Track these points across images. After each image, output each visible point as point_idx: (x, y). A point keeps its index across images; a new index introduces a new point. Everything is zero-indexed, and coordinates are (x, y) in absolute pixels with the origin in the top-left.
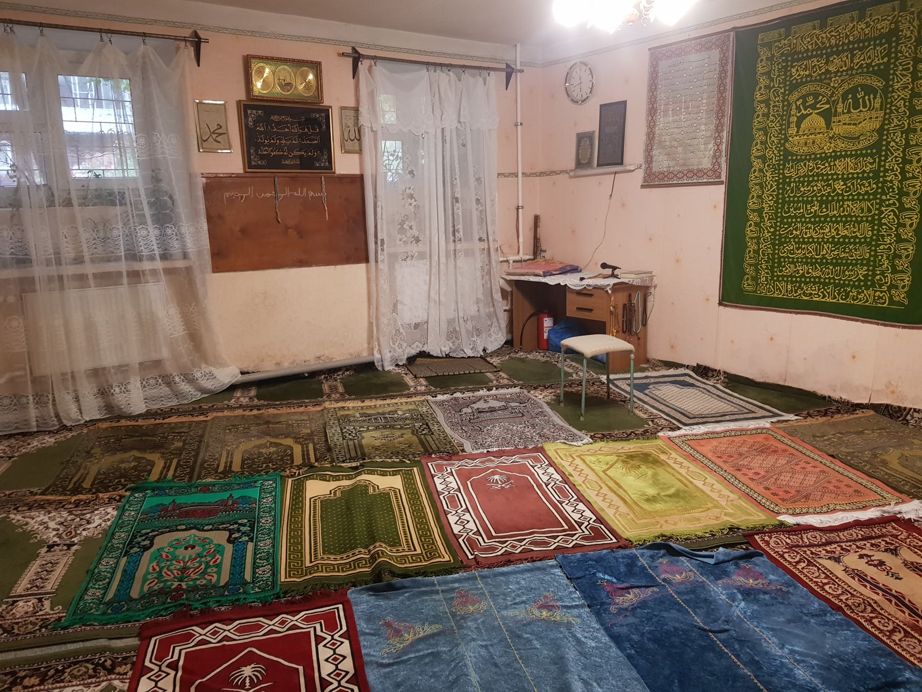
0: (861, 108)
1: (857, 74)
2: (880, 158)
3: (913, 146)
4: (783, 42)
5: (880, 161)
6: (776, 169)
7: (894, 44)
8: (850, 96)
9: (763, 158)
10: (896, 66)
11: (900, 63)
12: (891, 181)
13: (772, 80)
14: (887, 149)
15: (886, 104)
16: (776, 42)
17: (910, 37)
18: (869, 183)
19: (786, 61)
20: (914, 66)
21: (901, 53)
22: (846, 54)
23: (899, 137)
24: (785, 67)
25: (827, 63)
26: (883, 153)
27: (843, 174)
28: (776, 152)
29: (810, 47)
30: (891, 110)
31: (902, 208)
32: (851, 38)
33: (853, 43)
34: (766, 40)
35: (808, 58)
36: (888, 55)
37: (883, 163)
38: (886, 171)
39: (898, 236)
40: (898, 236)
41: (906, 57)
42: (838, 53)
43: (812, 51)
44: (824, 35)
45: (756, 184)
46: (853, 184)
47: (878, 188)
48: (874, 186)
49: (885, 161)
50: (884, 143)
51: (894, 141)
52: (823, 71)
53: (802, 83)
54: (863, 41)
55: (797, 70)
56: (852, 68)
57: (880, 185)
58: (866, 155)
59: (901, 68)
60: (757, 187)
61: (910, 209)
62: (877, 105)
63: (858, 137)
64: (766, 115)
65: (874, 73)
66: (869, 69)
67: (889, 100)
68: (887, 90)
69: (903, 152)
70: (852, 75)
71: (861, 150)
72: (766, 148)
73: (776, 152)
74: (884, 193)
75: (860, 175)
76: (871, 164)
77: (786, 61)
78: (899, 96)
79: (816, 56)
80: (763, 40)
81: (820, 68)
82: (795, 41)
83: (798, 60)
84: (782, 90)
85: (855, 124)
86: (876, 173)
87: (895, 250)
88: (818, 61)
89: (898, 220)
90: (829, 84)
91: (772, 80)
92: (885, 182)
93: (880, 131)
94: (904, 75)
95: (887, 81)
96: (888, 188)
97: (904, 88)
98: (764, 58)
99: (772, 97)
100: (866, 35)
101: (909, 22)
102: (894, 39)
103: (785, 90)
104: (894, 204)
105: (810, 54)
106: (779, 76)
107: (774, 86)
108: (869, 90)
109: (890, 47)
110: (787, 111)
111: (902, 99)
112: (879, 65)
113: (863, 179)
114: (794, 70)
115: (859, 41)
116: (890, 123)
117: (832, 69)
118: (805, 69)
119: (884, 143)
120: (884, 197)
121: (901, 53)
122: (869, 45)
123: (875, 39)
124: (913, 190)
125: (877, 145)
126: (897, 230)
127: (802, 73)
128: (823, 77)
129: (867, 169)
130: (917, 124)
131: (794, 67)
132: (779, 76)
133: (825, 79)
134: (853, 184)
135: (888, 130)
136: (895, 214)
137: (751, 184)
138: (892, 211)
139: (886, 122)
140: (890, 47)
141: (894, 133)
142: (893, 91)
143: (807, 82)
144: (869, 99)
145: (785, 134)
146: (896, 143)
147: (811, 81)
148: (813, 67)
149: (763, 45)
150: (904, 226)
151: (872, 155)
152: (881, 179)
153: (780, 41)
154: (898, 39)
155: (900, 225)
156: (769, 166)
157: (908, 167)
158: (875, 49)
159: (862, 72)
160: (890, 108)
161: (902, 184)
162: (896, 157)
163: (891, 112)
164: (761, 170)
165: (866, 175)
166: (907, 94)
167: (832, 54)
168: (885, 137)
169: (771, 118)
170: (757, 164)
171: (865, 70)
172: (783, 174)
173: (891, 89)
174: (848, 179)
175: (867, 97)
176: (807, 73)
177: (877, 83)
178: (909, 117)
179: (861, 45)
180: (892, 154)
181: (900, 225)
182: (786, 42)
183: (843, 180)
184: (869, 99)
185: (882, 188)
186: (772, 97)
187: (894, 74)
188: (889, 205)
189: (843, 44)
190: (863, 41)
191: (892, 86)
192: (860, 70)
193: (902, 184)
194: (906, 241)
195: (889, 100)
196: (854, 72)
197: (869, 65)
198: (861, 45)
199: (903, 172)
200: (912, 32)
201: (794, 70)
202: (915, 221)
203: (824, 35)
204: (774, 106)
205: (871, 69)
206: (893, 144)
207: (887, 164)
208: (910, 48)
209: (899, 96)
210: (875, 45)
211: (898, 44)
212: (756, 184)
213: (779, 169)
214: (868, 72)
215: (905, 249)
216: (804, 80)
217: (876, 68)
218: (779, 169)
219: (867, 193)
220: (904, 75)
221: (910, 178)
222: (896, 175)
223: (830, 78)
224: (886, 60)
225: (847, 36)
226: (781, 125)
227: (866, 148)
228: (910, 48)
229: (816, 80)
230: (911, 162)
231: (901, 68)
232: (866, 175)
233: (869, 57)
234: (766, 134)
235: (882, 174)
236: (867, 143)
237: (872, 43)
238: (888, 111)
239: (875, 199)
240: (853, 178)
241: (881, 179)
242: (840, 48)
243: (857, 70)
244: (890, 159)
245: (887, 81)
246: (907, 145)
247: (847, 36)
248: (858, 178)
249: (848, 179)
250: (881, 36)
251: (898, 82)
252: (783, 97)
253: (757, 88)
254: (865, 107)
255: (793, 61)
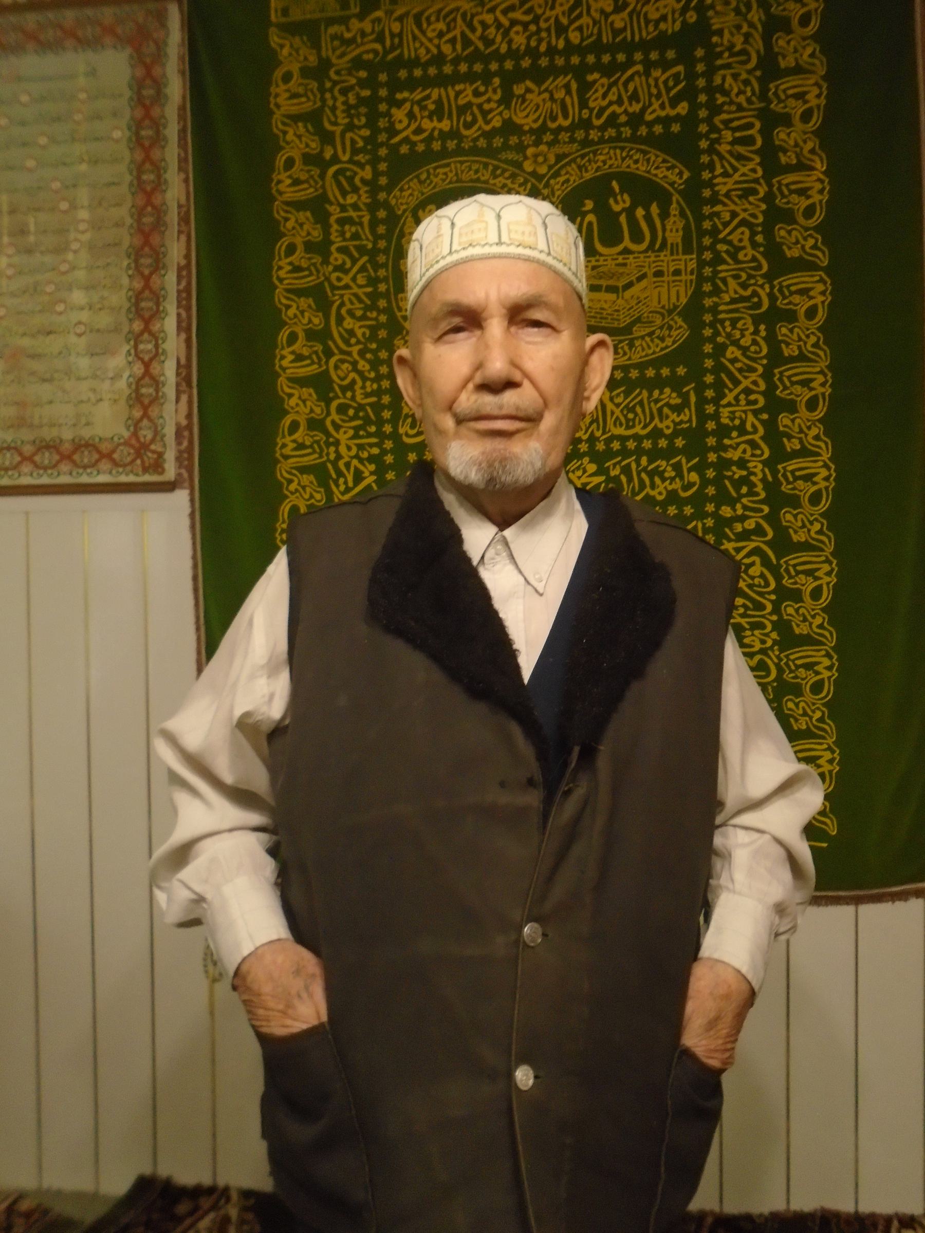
0: (627, 242)
1: (602, 141)
2: (701, 388)
3: (792, 359)
4: (355, 24)
5: (702, 401)
6: (367, 421)
7: (700, 68)
8: (589, 205)
9: (321, 384)
10: (713, 129)
11: (726, 123)
12: (742, 463)
13: (327, 138)
14: (719, 368)
15: (702, 233)
16: (331, 21)
17: (743, 52)
18: (677, 467)
19: (371, 83)
20: (766, 132)
21: (726, 93)
22: (561, 81)
23: (748, 333)
24: (371, 103)
25: (506, 100)
26: (709, 379)
27: (592, 440)
28: (363, 365)
29: (447, 49)
30: (717, 254)
31: (783, 544)
32: (575, 37)
33: (581, 50)
34: (296, 15)
35: (443, 81)
36: (689, 94)
37: (710, 409)
38: (723, 431)
39: (783, 626)
40: (783, 626)
41: (740, 108)
42: (538, 75)
43: (456, 61)
44: (489, 18)
45: (303, 470)
46: (626, 470)
47: (705, 482)
48: (694, 477)
49: (716, 401)
50: (708, 348)
51: (736, 343)
52: (497, 123)
53: (430, 156)
54: (612, 49)
55: (411, 115)
56: (586, 124)
57: (711, 474)
58: (658, 383)
59: (728, 135)
60: (306, 479)
61: (806, 547)
62: (675, 237)
63: (628, 330)
64: (320, 248)
65: (651, 140)
66: (634, 130)
67: (707, 225)
68: (695, 195)
69: (767, 375)
70: (586, 143)
71: (642, 366)
72: (329, 354)
73: (363, 365)
74: (723, 498)
75: (647, 444)
76: (678, 409)
77: (371, 83)
78: (734, 215)
79: (470, 77)
80: (285, 12)
81: (485, 113)
82: (396, 27)
83: (411, 84)
84: (367, 173)
85: (612, 289)
86: (695, 442)
87: (780, 670)
88: (477, 93)
89: (778, 578)
90: (519, 165)
91: (327, 138)
92: (723, 464)
93: (693, 312)
94: (740, 157)
95: (695, 168)
96: (738, 484)
97: (747, 193)
98: (295, 68)
99: (333, 192)
100: (616, 32)
101: (737, 11)
102: (700, 53)
103: (376, 174)
104: (759, 531)
105: (448, 69)
106: (350, 127)
107: (335, 159)
108: (645, 191)
109: (691, 76)
110: (388, 236)
111: (743, 223)
112: (666, 121)
113: (654, 454)
114: (399, 114)
115: (598, 47)
116: (716, 292)
117: (525, 118)
118: (438, 113)
119: (708, 348)
120: (726, 512)
121: (726, 93)
122: (630, 63)
123: (645, 46)
124: (806, 490)
125: (688, 353)
126: (776, 610)
127: (427, 124)
128: (498, 142)
129: (667, 426)
130: (796, 299)
131: (399, 104)
132: (350, 127)
133: (506, 147)
134: (626, 470)
135: (714, 310)
136: (766, 562)
137: (283, 471)
138: (756, 551)
139: (707, 287)
140: (691, 76)
141: (734, 322)
142: (714, 200)
143: (444, 153)
144: (648, 218)
145: (388, 311)
146: (745, 350)
147: (459, 151)
148: (462, 110)
149: (292, 29)
150: (796, 596)
151: (676, 384)
152: (712, 457)
153: (344, 21)
154: (712, 55)
155: (786, 594)
156: (342, 409)
157: (784, 420)
158: (647, 74)
159: (618, 138)
160: (712, 248)
161: (775, 473)
162: (747, 391)
163: (718, 260)
164: (315, 424)
165: (663, 443)
166: (755, 209)
167: (519, 75)
168: (708, 332)
169: (337, 258)
170: (300, 404)
171: (627, 132)
172: (395, 436)
173: (707, 193)
174: (609, 454)
175: (640, 212)
176: (445, 125)
177: (668, 173)
178: (770, 277)
179: (606, 58)
180: (736, 383)
181: (786, 594)
182: (367, 26)
183: (596, 457)
184: (648, 218)
185: (718, 481)
186: (333, 192)
187: (711, 150)
188: (745, 535)
189: (552, 51)
190: (612, 49)
191: (710, 184)
192: (611, 132)
193: (775, 473)
194: (808, 640)
195: (707, 225)
196: (594, 135)
197: (636, 120)
198: (606, 58)
199: (774, 436)
200: (747, 36)
201: (399, 114)
202: (827, 581)
203: (489, 18)
204: (342, 222)
205: (643, 131)
206: (732, 352)
207: (725, 412)
208: (746, 82)
209: (734, 215)
210: (648, 65)
211: (709, 74)
212: (303, 470)
213: (380, 422)
214: (634, 139)
215: (809, 667)
216: (436, 146)
217: (658, 129)
218: (380, 422)
219: (672, 497)
220: (740, 157)
221: (796, 454)
222: (753, 444)
223: (521, 148)
224: (683, 108)
225: (561, 30)
226: (373, 281)
227: (656, 363)
228: (746, 82)
229: (475, 151)
230: (791, 407)
231: (728, 135)
232: (663, 443)
233: (634, 97)
234: (323, 305)
235: (711, 441)
236: (656, 349)
237: (638, 56)
238: (708, 256)
239: (700, 514)
240: (625, 453)
241: (712, 457)
242: (544, 62)
243: (602, 128)
244: (730, 397)
245: (695, 168)
246: (776, 358)
247: (561, 30)
248: (639, 452)
249: (609, 454)
250: (662, 42)
251: (725, 174)
252: (373, 193)
253: (280, 161)
254: (637, 237)
255: (395, 86)
